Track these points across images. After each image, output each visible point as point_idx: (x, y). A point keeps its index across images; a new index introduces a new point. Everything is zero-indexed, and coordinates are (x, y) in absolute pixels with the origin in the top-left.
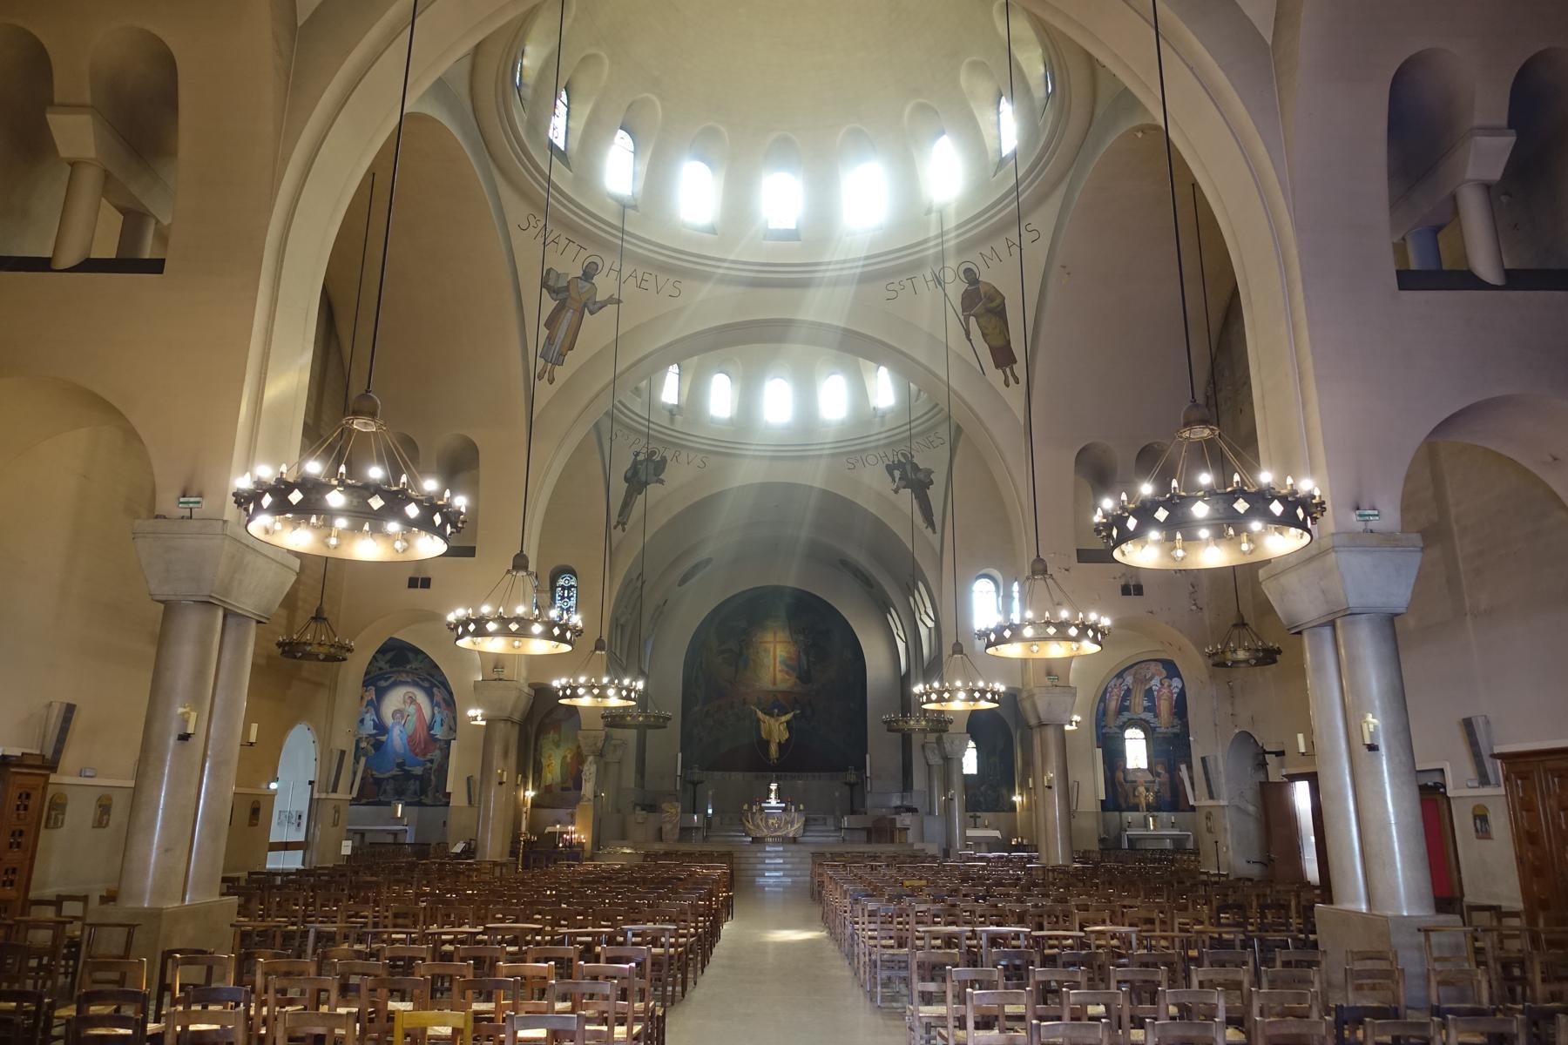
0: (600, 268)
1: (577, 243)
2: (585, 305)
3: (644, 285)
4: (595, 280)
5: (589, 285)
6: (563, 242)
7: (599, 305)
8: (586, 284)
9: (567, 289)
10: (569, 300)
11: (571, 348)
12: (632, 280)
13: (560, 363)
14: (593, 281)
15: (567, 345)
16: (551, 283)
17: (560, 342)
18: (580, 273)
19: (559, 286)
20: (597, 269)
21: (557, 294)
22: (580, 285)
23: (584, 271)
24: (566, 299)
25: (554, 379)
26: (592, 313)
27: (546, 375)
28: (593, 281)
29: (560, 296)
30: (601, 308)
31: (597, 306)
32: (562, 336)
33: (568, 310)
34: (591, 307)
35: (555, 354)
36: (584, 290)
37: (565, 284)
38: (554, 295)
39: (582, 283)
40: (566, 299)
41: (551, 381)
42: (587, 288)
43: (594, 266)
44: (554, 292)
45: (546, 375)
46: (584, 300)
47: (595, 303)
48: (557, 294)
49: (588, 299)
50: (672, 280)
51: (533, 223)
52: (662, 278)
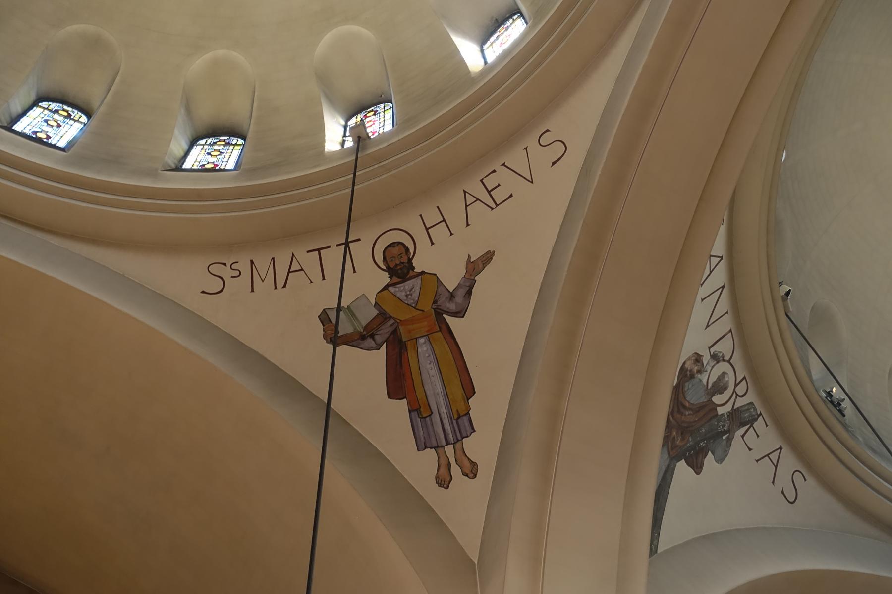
0: (412, 251)
1: (334, 246)
2: (439, 313)
3: (498, 195)
4: (419, 265)
5: (417, 282)
6: (310, 261)
7: (462, 292)
8: (408, 284)
9: (383, 316)
10: (402, 329)
11: (469, 390)
12: (477, 210)
13: (469, 429)
14: (418, 270)
15: (457, 391)
16: (345, 328)
17: (441, 400)
18: (385, 278)
19: (364, 323)
20: (407, 249)
21: (372, 336)
22: (402, 295)
23: (391, 271)
24: (395, 332)
25: (474, 465)
26: (460, 313)
27: (455, 470)
28: (418, 270)
29: (378, 338)
30: (469, 293)
31: (459, 299)
32: (439, 388)
33: (416, 347)
34: (452, 307)
35: (447, 426)
36: (415, 295)
37: (375, 312)
38: (369, 342)
39: (401, 290)
40: (395, 332)
41: (471, 471)
42: (417, 289)
43: (396, 251)
44: (363, 337)
45: (455, 470)
46: (427, 306)
47: (452, 296)
48: (372, 336)
49: (435, 302)
50: (531, 142)
51: (226, 273)
52: (516, 158)
